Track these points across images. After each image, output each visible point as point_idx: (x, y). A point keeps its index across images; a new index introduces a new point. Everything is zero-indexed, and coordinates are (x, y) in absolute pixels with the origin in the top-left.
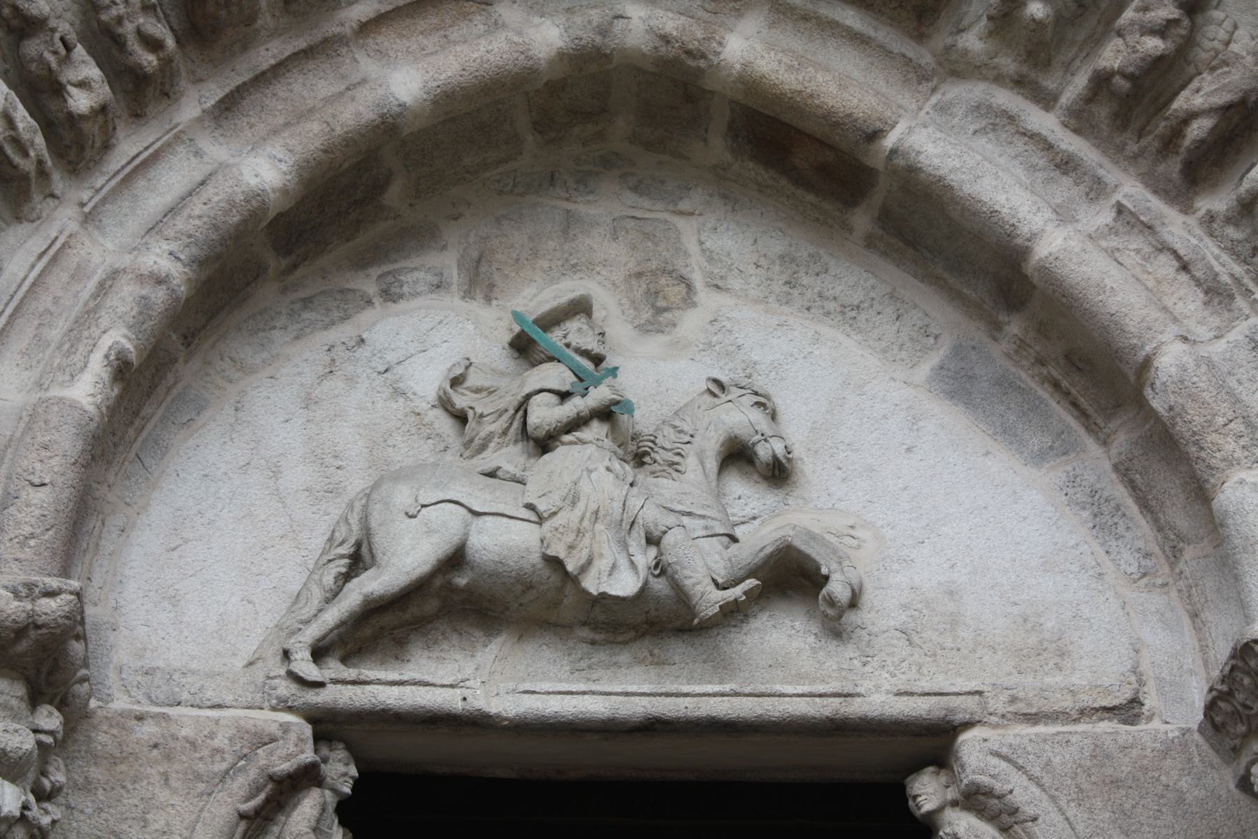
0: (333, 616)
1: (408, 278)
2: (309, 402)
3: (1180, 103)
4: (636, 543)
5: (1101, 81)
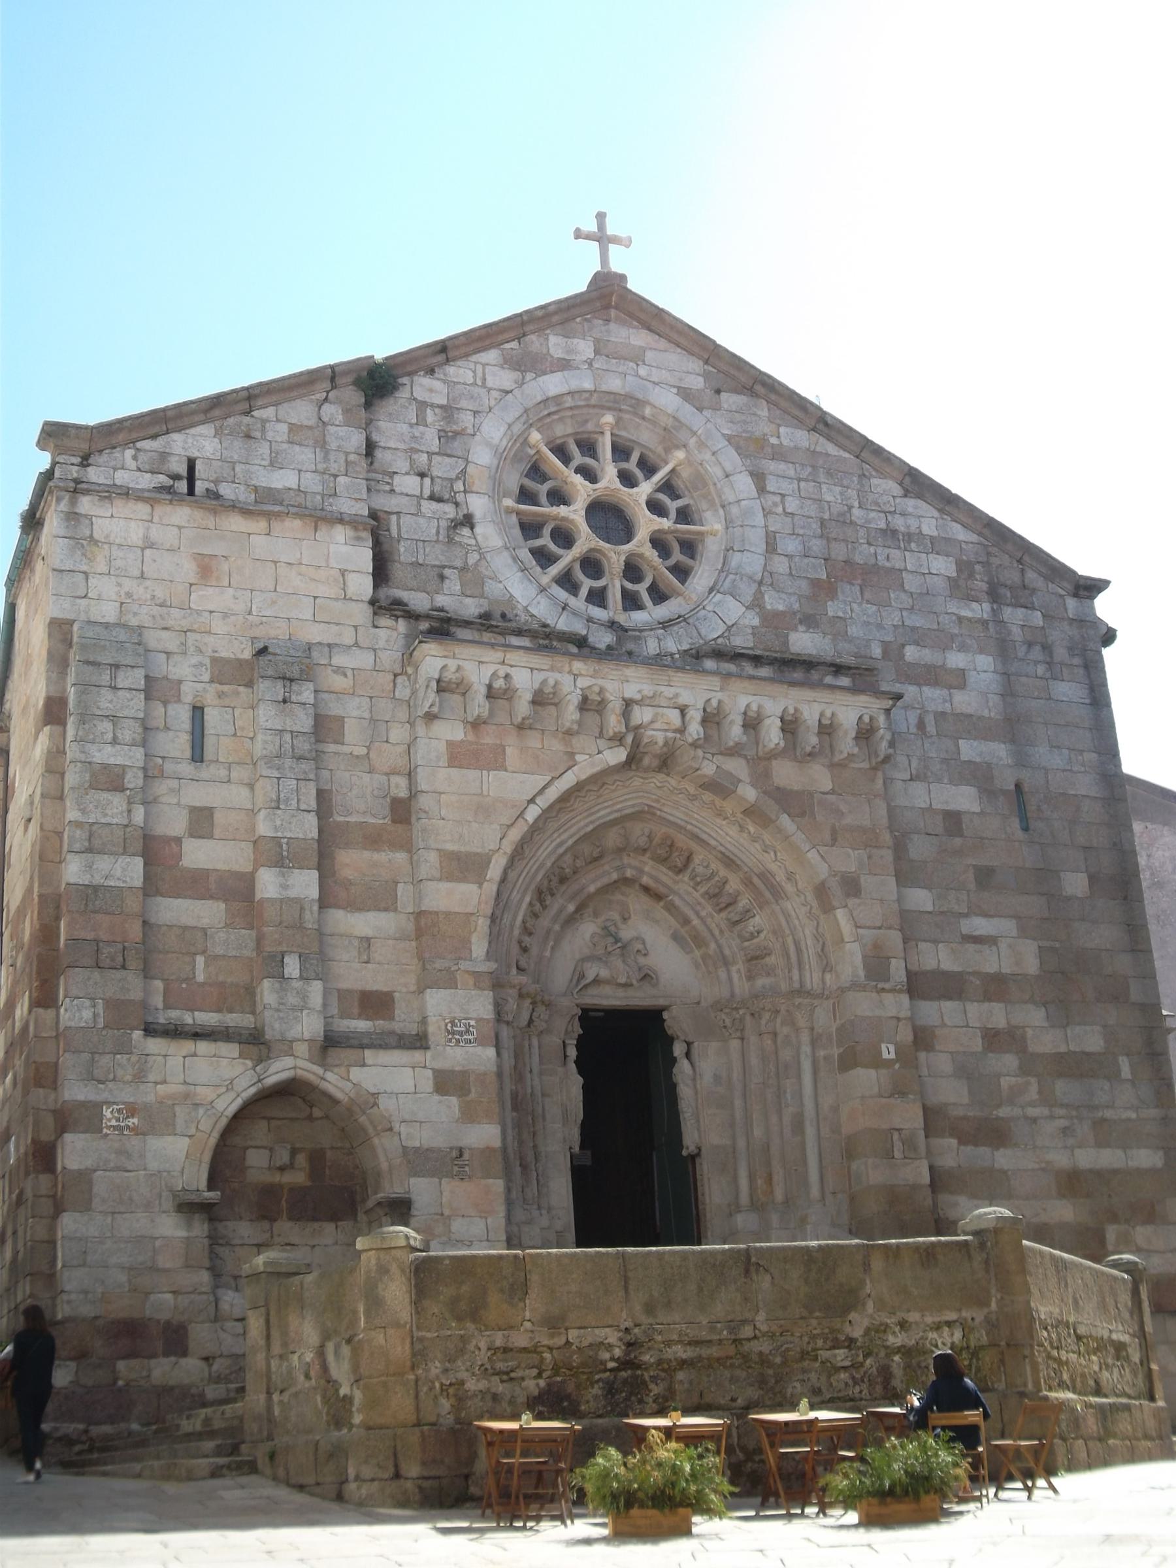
5: (707, 893)
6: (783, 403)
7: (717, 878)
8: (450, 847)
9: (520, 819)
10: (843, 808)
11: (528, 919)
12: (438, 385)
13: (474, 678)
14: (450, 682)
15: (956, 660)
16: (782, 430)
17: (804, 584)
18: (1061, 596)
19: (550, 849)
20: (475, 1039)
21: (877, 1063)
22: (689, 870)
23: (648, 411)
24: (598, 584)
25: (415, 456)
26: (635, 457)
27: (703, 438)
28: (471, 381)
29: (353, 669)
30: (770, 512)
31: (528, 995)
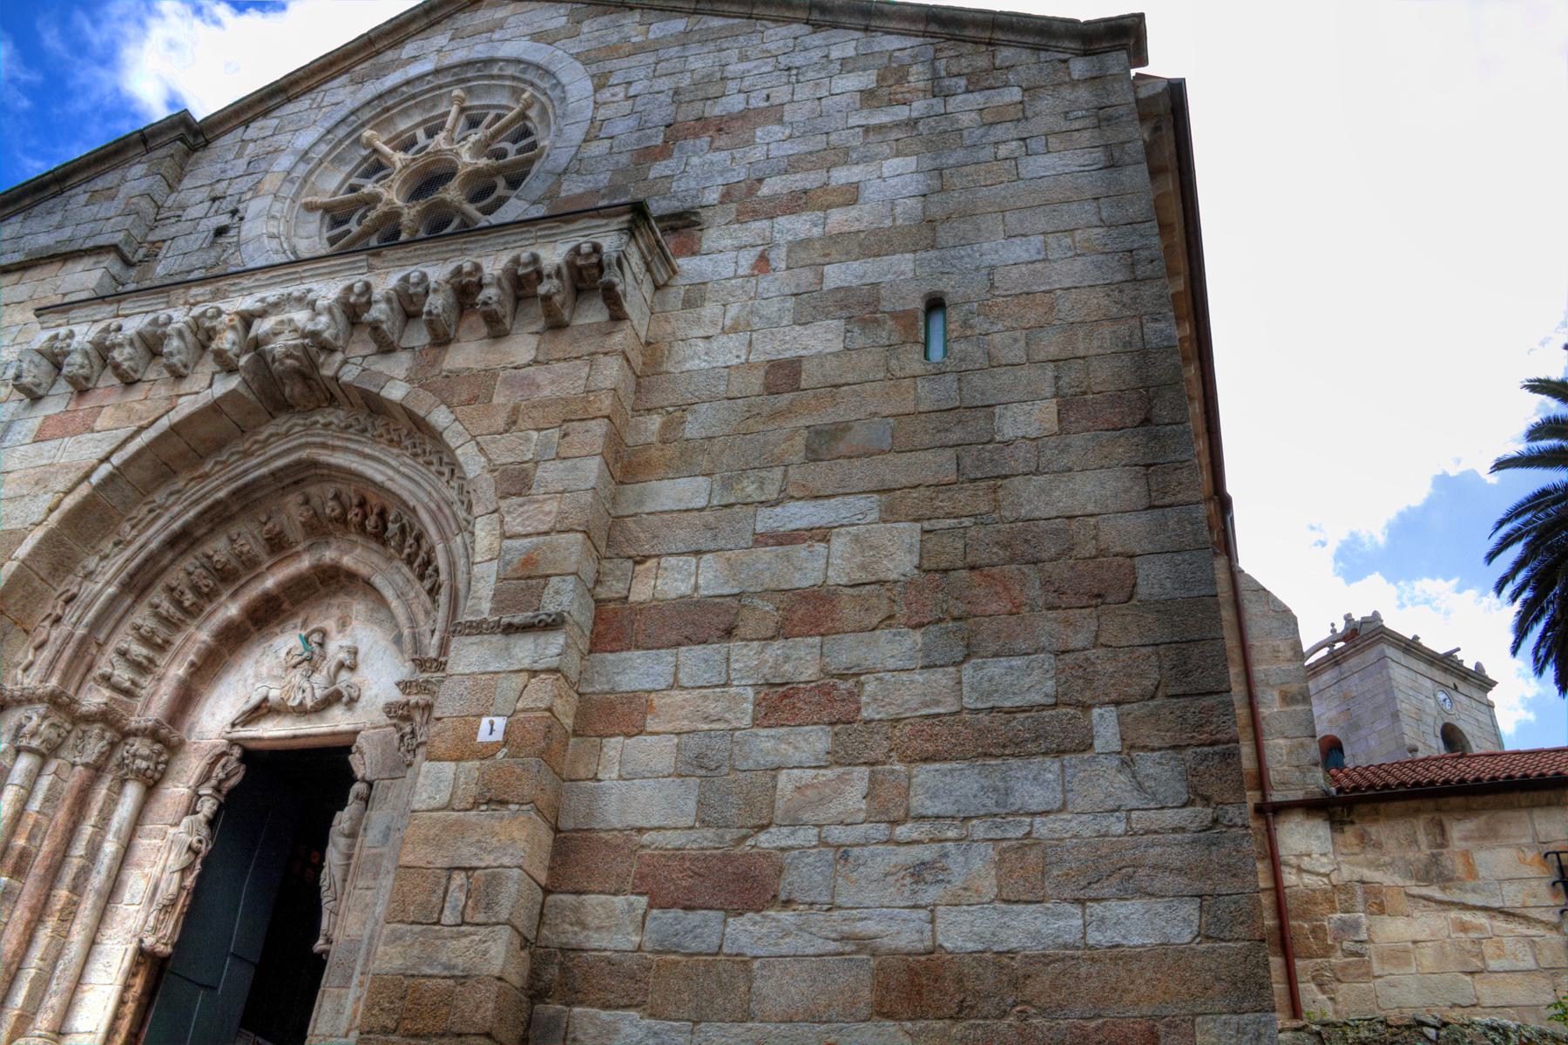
2: (257, 662)
15: (841, 176)
18: (1065, 61)
21: (466, 749)
23: (495, 71)
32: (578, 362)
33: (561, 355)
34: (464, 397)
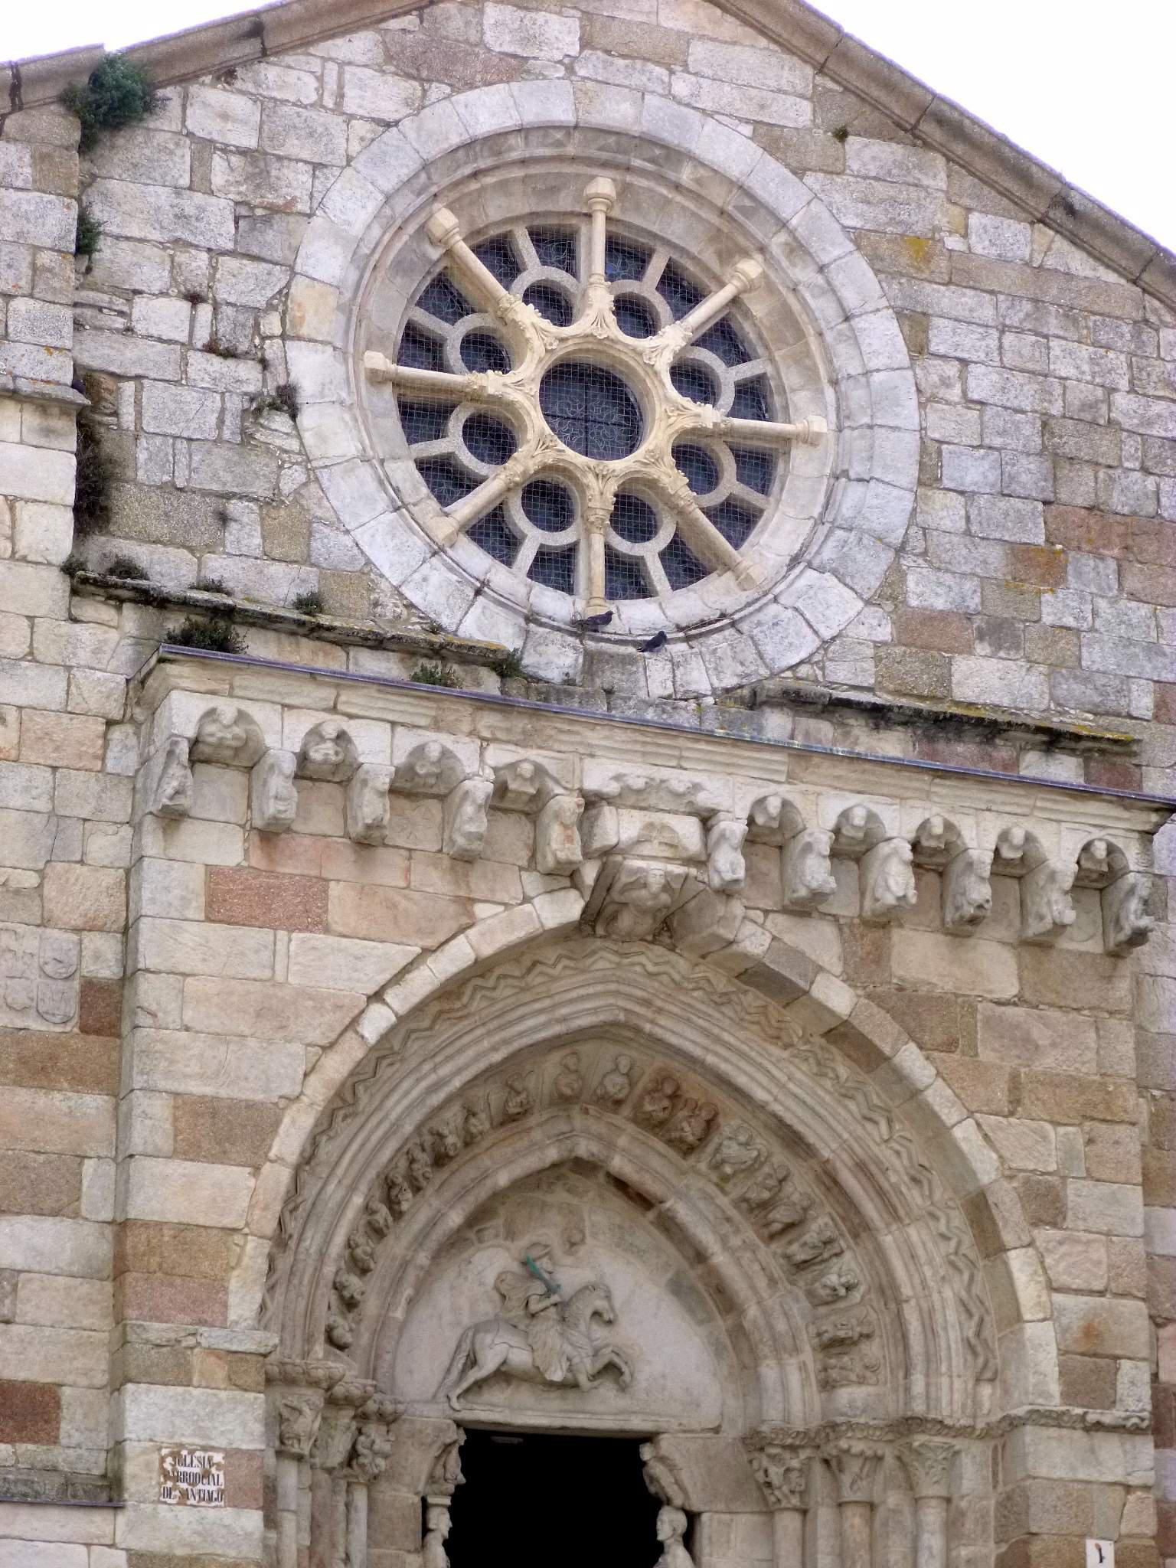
0: (465, 1385)
1: (486, 1233)
3: (771, 1216)
4: (564, 1359)
6: (981, 164)
7: (766, 1169)
8: (196, 1088)
9: (350, 1034)
10: (1041, 1035)
11: (361, 1239)
12: (239, 104)
13: (270, 740)
14: (220, 744)
16: (975, 219)
17: (995, 556)
19: (415, 1093)
20: (221, 1492)
22: (711, 1148)
23: (686, 175)
24: (560, 539)
25: (182, 258)
26: (656, 269)
27: (801, 232)
28: (314, 97)
29: (20, 708)
30: (933, 399)
31: (348, 1401)
32: (1074, 1014)
33: (1051, 997)
34: (940, 1038)
